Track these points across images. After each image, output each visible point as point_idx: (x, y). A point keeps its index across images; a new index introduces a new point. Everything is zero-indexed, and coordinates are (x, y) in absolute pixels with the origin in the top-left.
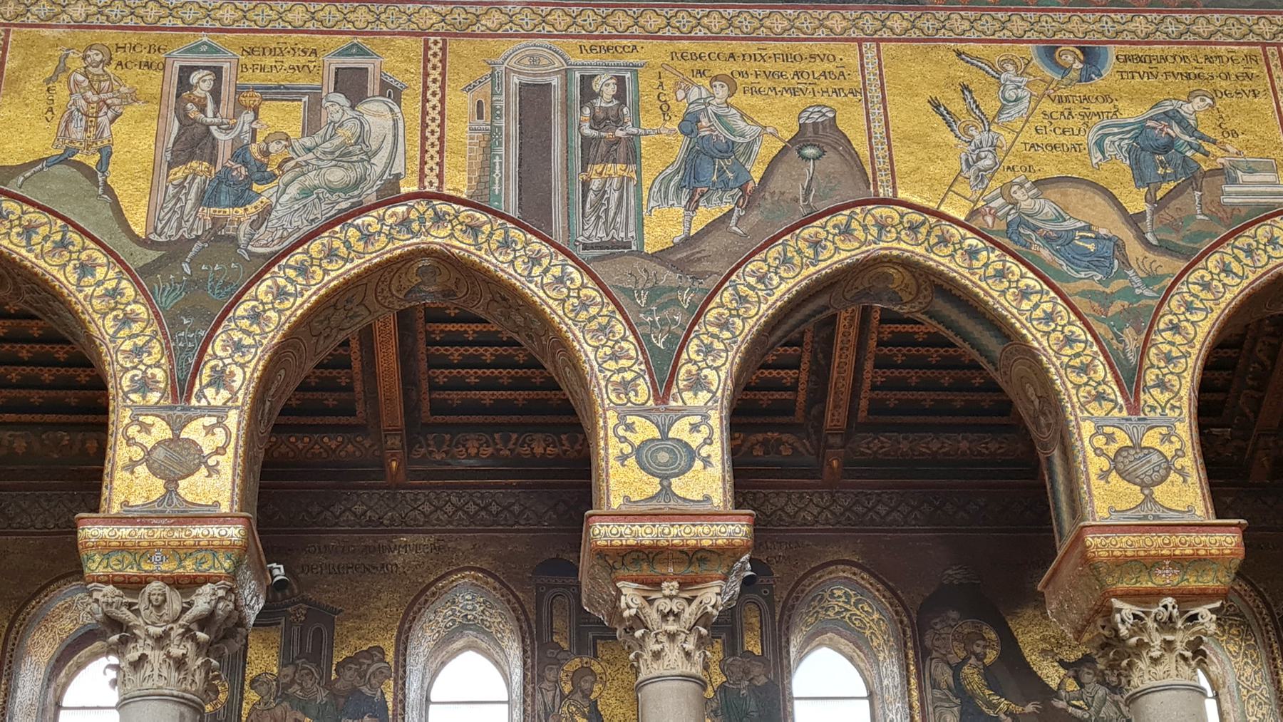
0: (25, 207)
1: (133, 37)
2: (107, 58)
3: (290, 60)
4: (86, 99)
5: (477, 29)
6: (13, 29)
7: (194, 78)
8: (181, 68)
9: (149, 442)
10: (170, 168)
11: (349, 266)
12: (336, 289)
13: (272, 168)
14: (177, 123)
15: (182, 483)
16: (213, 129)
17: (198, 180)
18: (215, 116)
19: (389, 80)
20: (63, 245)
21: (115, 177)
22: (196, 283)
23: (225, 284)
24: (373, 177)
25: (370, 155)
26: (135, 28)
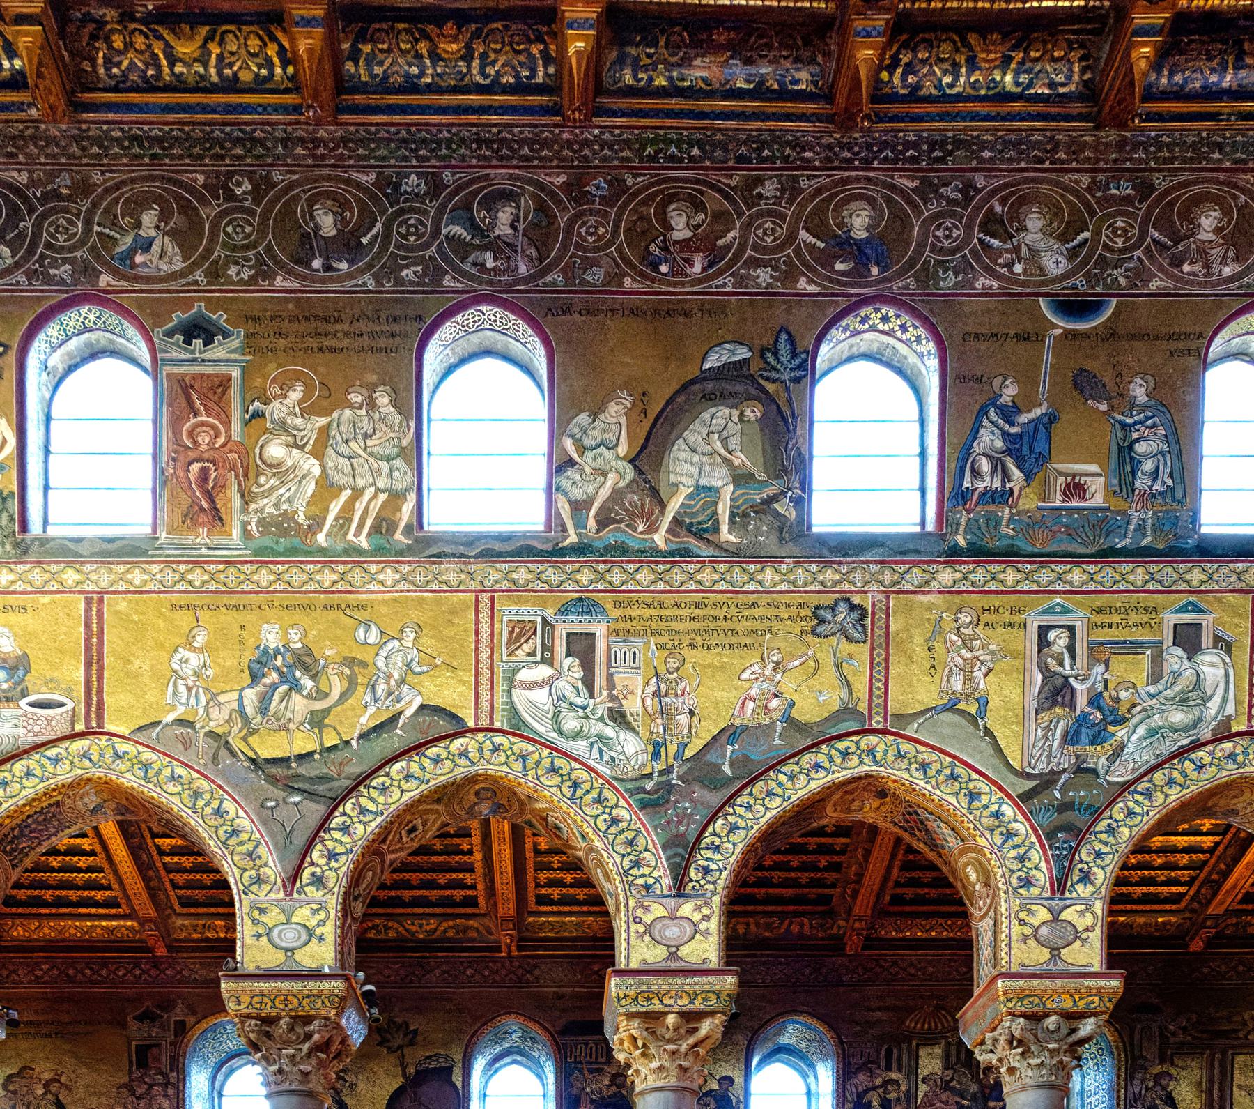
2: (975, 620)
3: (1134, 618)
4: (959, 655)
6: (892, 595)
7: (1052, 635)
8: (1040, 627)
11: (1185, 791)
12: (1172, 810)
13: (1122, 711)
14: (1040, 677)
16: (1071, 680)
17: (1062, 722)
18: (1072, 669)
19: (1221, 634)
21: (991, 720)
23: (1089, 806)
24: (1208, 719)
25: (1205, 700)
26: (996, 592)
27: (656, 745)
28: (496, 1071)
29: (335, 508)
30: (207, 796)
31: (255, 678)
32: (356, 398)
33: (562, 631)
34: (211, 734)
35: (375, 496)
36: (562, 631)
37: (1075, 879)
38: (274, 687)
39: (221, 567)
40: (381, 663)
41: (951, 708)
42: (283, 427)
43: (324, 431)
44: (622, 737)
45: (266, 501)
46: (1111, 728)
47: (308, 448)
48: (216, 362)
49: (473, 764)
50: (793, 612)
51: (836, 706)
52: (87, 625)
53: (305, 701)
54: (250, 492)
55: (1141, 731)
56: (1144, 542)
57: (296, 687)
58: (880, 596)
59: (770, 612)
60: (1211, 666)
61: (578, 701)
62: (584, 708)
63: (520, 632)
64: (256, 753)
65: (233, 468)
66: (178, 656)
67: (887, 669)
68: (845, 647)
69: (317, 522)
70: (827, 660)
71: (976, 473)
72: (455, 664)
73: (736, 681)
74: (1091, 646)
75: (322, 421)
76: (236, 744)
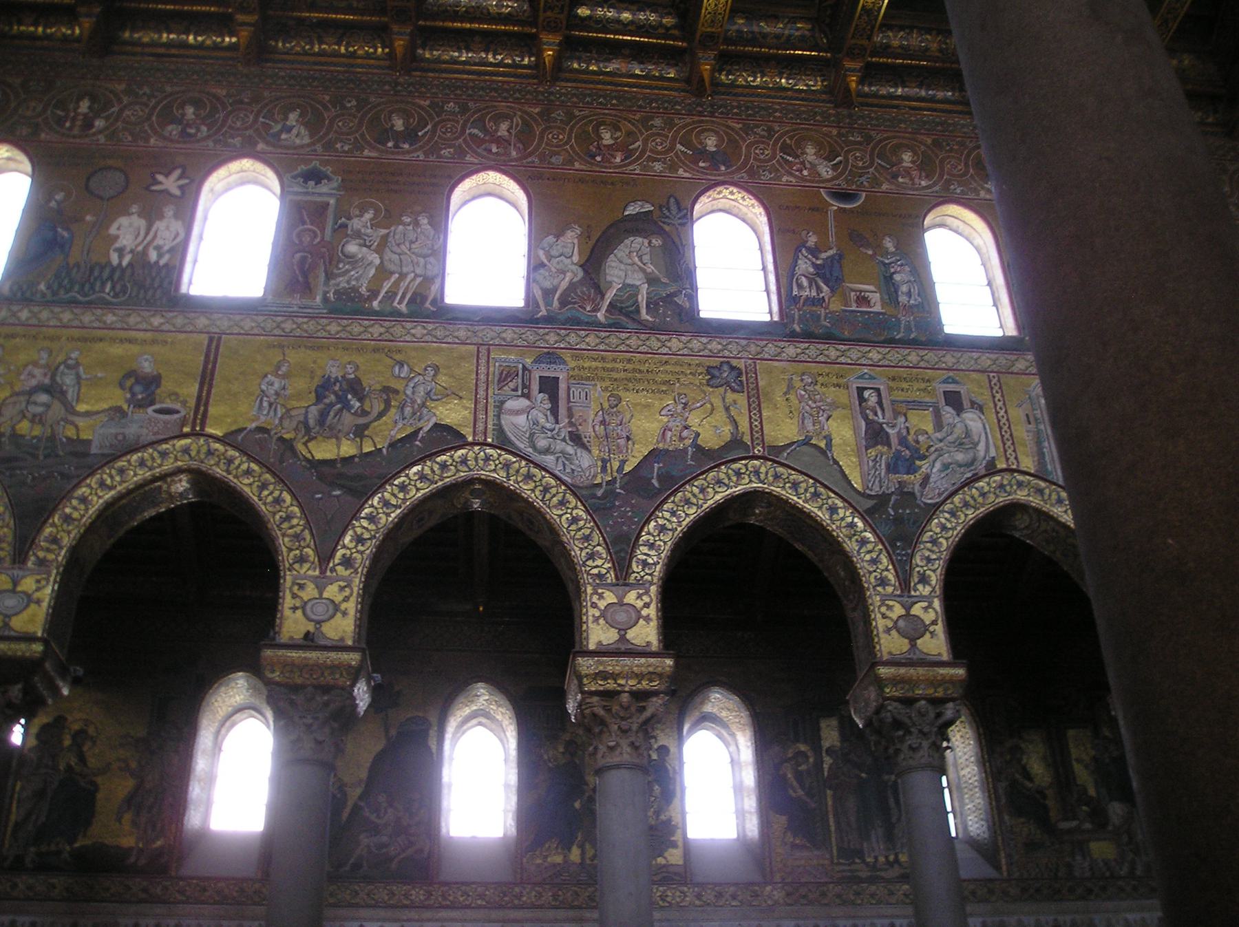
0: (790, 471)
1: (826, 369)
5: (1015, 369)
9: (894, 616)
10: (867, 450)
15: (919, 642)
20: (816, 495)
22: (898, 520)
27: (604, 461)
28: (463, 733)
29: (387, 286)
30: (271, 487)
31: (319, 398)
32: (407, 220)
33: (536, 375)
34: (281, 439)
35: (413, 280)
36: (536, 375)
37: (916, 580)
38: (331, 405)
39: (305, 320)
40: (409, 392)
41: (806, 442)
42: (358, 235)
43: (385, 239)
44: (579, 455)
45: (341, 279)
46: (918, 463)
47: (373, 247)
48: (320, 194)
49: (471, 470)
50: (693, 369)
51: (728, 438)
52: (207, 356)
53: (353, 417)
54: (332, 273)
55: (938, 465)
56: (912, 336)
57: (347, 406)
58: (750, 361)
59: (678, 369)
60: (972, 420)
61: (548, 425)
62: (552, 430)
63: (505, 377)
64: (313, 457)
65: (323, 257)
66: (267, 380)
67: (760, 411)
68: (730, 396)
69: (374, 294)
70: (717, 402)
71: (800, 286)
72: (461, 394)
73: (658, 416)
74: (893, 402)
75: (384, 232)
76: (300, 447)
